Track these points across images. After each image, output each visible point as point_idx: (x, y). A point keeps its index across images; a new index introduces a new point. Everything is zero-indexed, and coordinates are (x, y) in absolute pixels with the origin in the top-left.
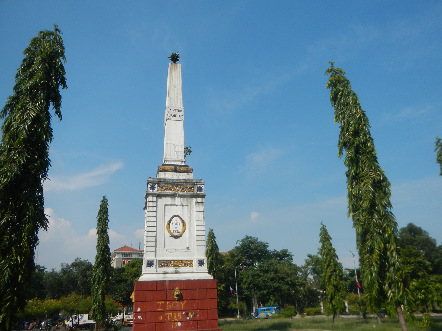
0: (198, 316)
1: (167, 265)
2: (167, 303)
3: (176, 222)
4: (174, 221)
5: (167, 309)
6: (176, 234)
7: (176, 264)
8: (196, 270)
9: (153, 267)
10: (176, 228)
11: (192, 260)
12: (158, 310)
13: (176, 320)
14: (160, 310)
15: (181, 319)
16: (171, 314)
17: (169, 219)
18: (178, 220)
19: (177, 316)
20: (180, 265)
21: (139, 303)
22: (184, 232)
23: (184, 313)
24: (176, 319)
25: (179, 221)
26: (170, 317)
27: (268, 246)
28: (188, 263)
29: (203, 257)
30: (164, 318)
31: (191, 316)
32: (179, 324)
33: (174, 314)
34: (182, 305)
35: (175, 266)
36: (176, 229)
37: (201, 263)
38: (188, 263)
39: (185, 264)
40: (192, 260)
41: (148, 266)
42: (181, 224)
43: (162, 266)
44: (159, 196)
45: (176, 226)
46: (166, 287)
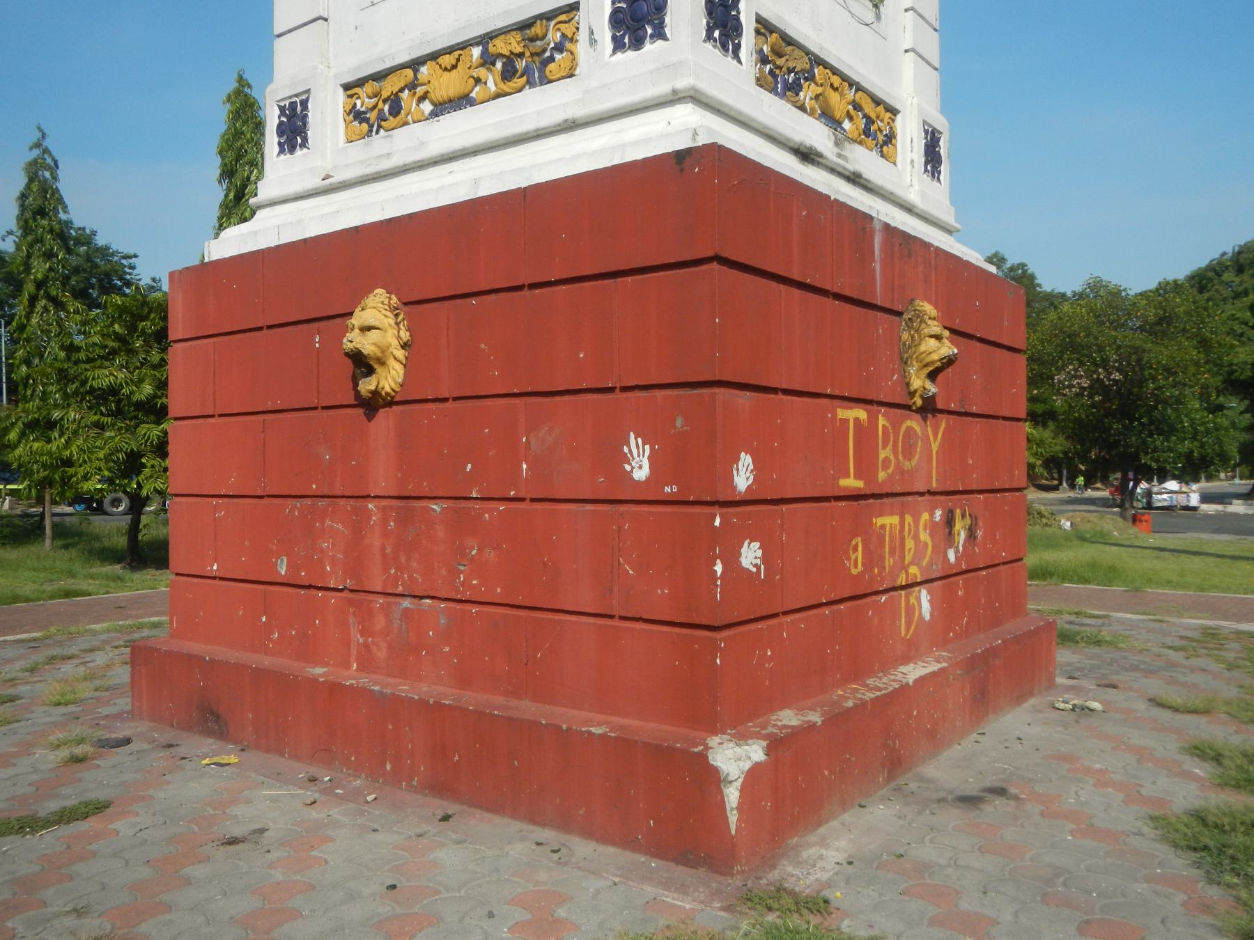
0: (980, 534)
1: (795, 88)
2: (882, 421)
5: (882, 475)
7: (834, 97)
8: (923, 195)
9: (736, 56)
11: (894, 112)
12: (844, 482)
13: (913, 570)
14: (851, 483)
15: (930, 564)
16: (895, 520)
19: (916, 538)
20: (847, 125)
21: (744, 399)
23: (938, 514)
24: (912, 563)
26: (892, 553)
27: (132, 268)
30: (872, 559)
31: (963, 535)
32: (924, 601)
33: (908, 519)
34: (935, 447)
35: (829, 117)
40: (894, 112)
41: (709, 37)
43: (773, 90)
46: (874, 270)
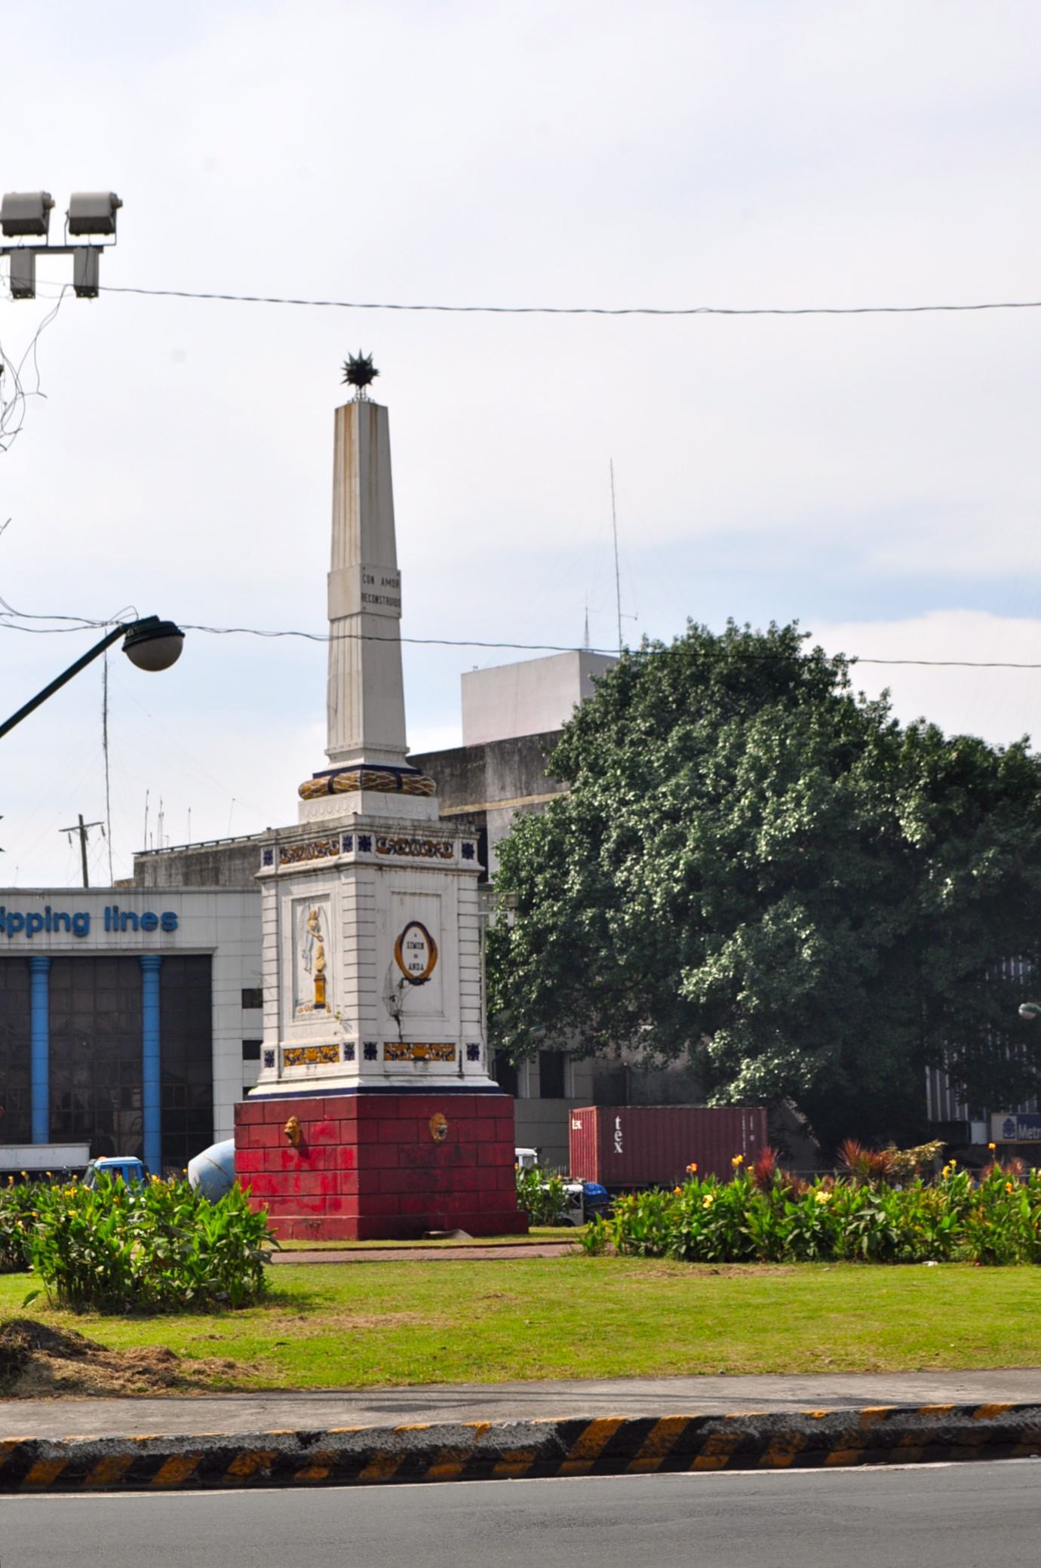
3: (415, 940)
4: (410, 937)
6: (416, 973)
10: (416, 956)
17: (401, 931)
18: (415, 935)
22: (430, 968)
25: (421, 938)
28: (445, 1052)
29: (475, 1033)
36: (416, 961)
37: (473, 1052)
38: (445, 1052)
39: (438, 1057)
42: (426, 946)
44: (380, 867)
45: (416, 951)
